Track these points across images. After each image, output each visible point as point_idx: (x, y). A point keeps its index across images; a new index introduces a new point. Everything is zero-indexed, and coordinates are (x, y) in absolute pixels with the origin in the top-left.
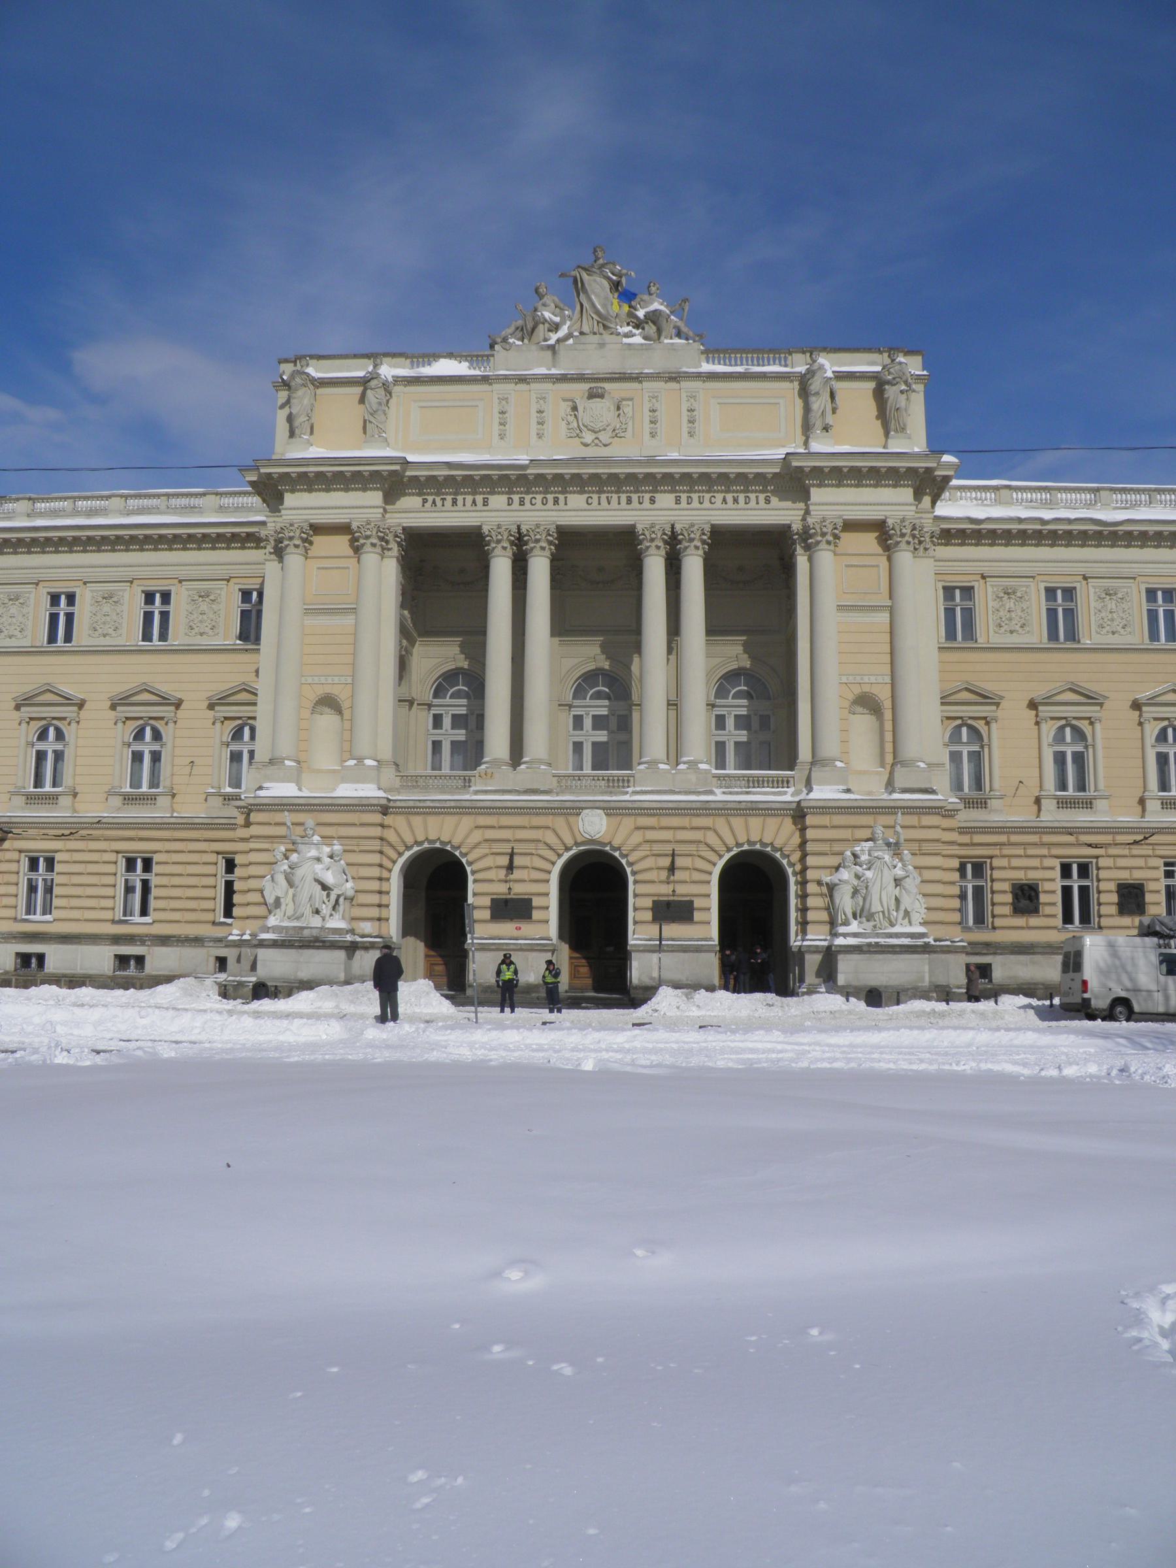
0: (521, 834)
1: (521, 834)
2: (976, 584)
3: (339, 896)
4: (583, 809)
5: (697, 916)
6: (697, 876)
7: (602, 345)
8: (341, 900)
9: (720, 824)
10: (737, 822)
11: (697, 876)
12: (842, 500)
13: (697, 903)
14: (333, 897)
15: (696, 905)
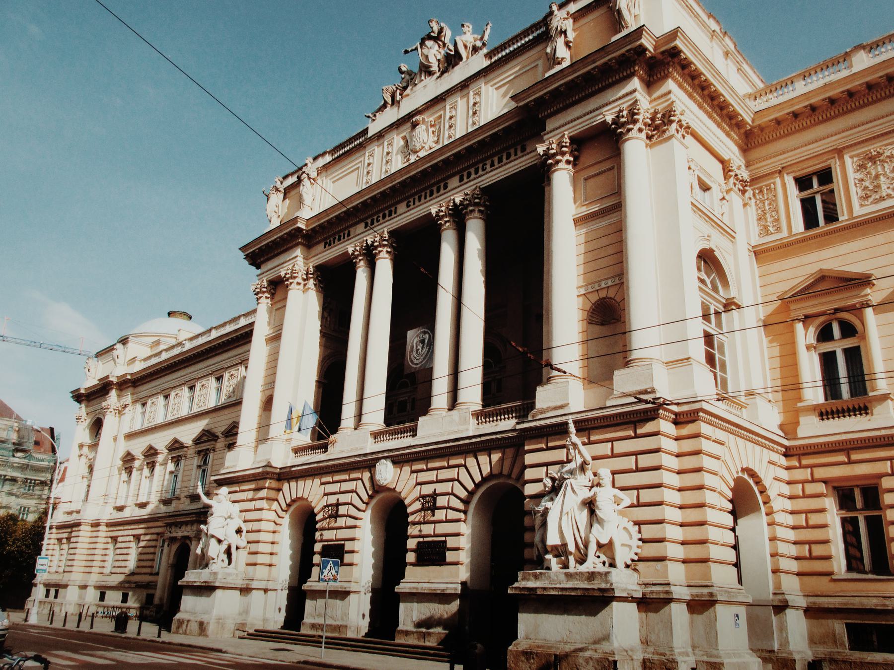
0: (345, 486)
1: (345, 486)
2: (831, 162)
3: (229, 547)
4: (379, 459)
5: (450, 556)
6: (452, 515)
7: (425, 86)
8: (233, 549)
9: (471, 462)
10: (483, 459)
11: (452, 515)
12: (569, 118)
13: (451, 542)
14: (224, 547)
15: (449, 545)
